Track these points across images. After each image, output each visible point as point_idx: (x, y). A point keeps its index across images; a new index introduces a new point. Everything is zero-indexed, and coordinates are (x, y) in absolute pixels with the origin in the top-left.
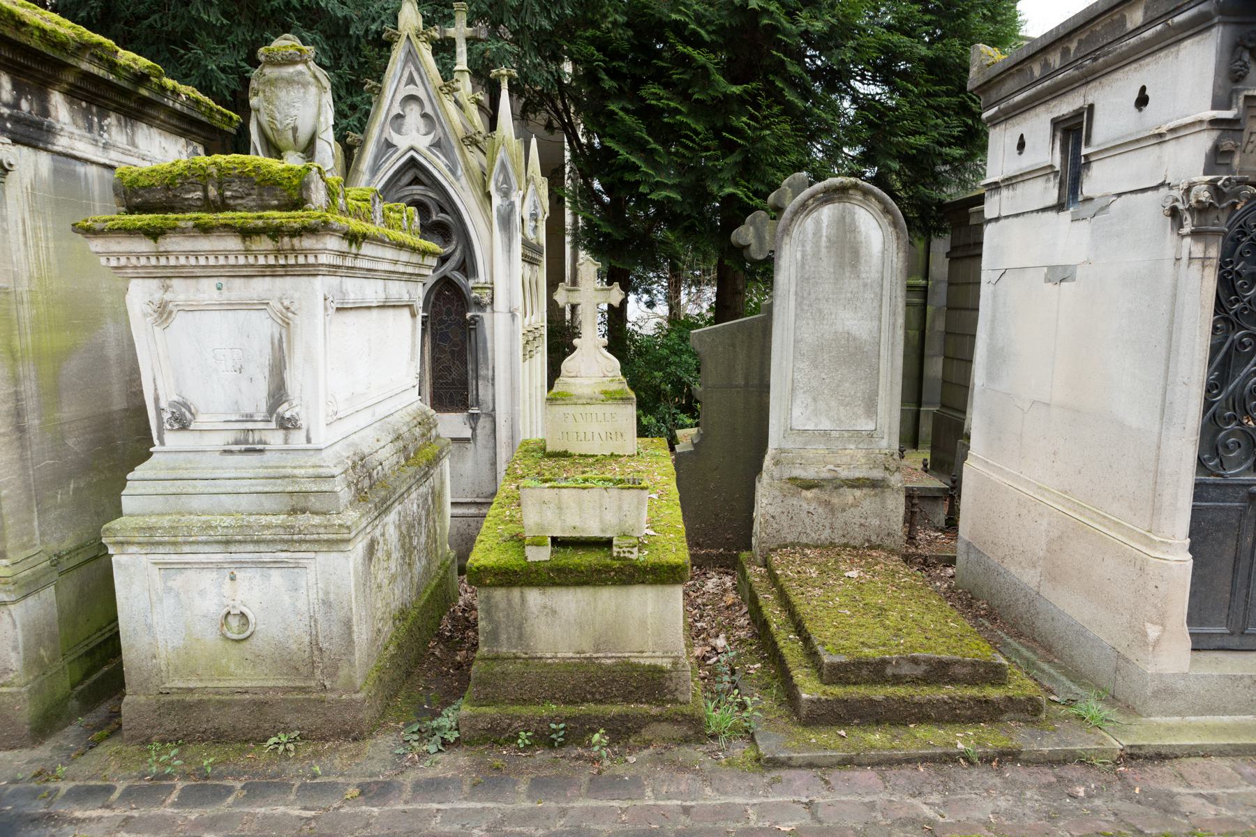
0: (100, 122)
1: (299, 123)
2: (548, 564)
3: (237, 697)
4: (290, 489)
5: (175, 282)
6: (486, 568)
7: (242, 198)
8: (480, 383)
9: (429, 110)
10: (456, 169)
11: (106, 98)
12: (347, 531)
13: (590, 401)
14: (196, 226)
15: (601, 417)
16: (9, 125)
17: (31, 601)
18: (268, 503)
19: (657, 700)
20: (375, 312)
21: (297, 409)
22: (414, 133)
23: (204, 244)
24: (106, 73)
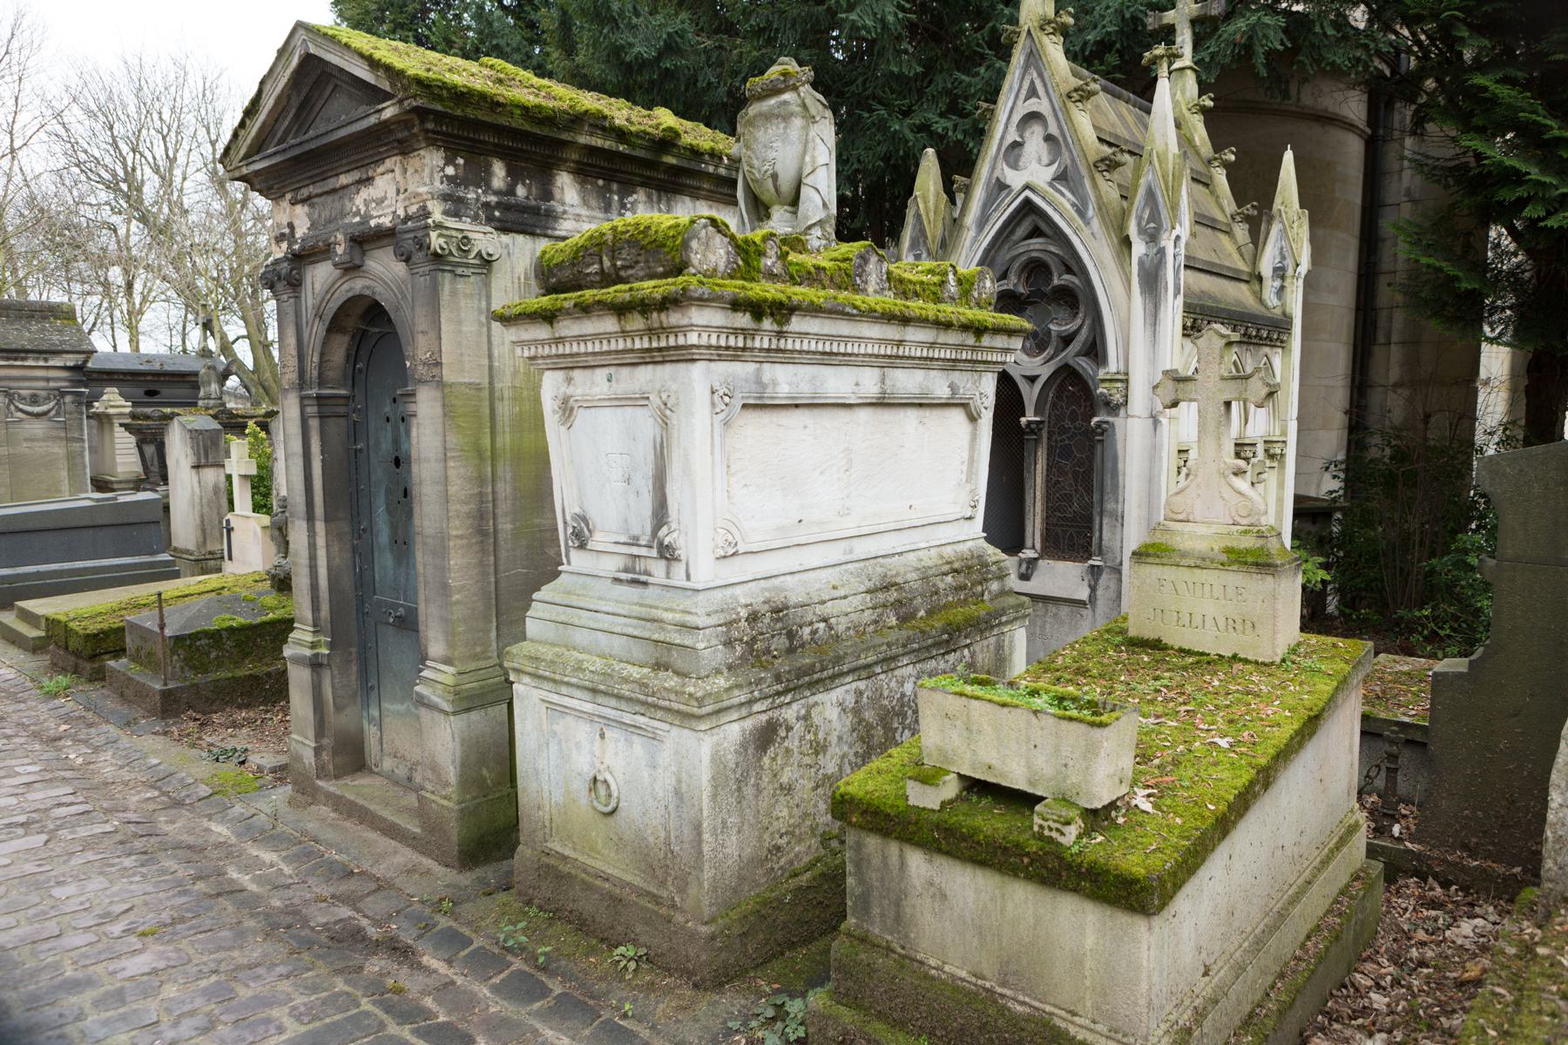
0: (621, 200)
1: (779, 168)
2: (935, 817)
3: (598, 882)
4: (656, 637)
5: (576, 374)
6: (852, 799)
7: (631, 267)
8: (1105, 521)
9: (1053, 129)
10: (1086, 209)
11: (630, 174)
12: (695, 704)
13: (1202, 562)
14: (576, 305)
15: (1218, 590)
16: (497, 214)
17: (475, 716)
18: (638, 651)
20: (864, 415)
21: (675, 535)
22: (1034, 166)
23: (589, 326)
24: (614, 144)
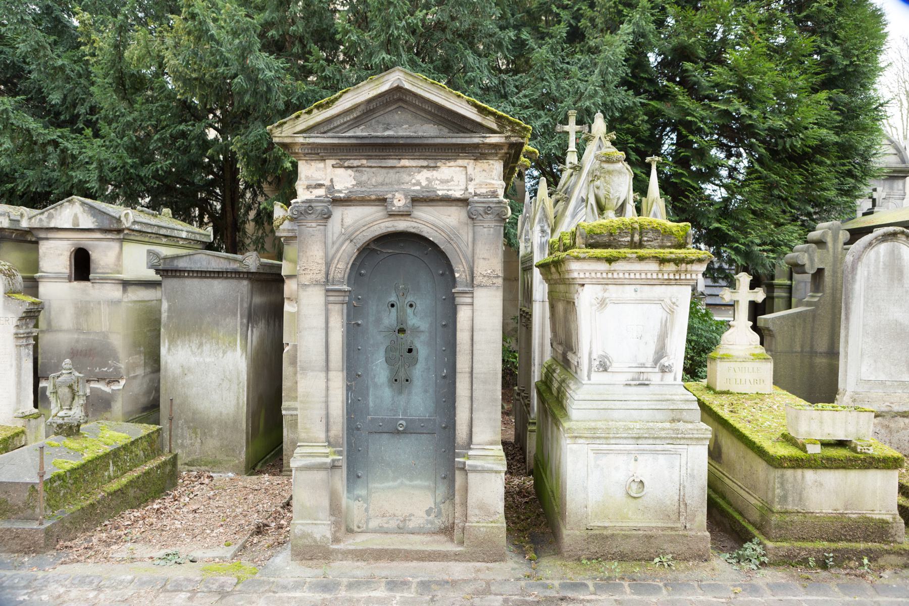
4: (671, 407)
15: (751, 370)
18: (659, 415)
19: (884, 541)
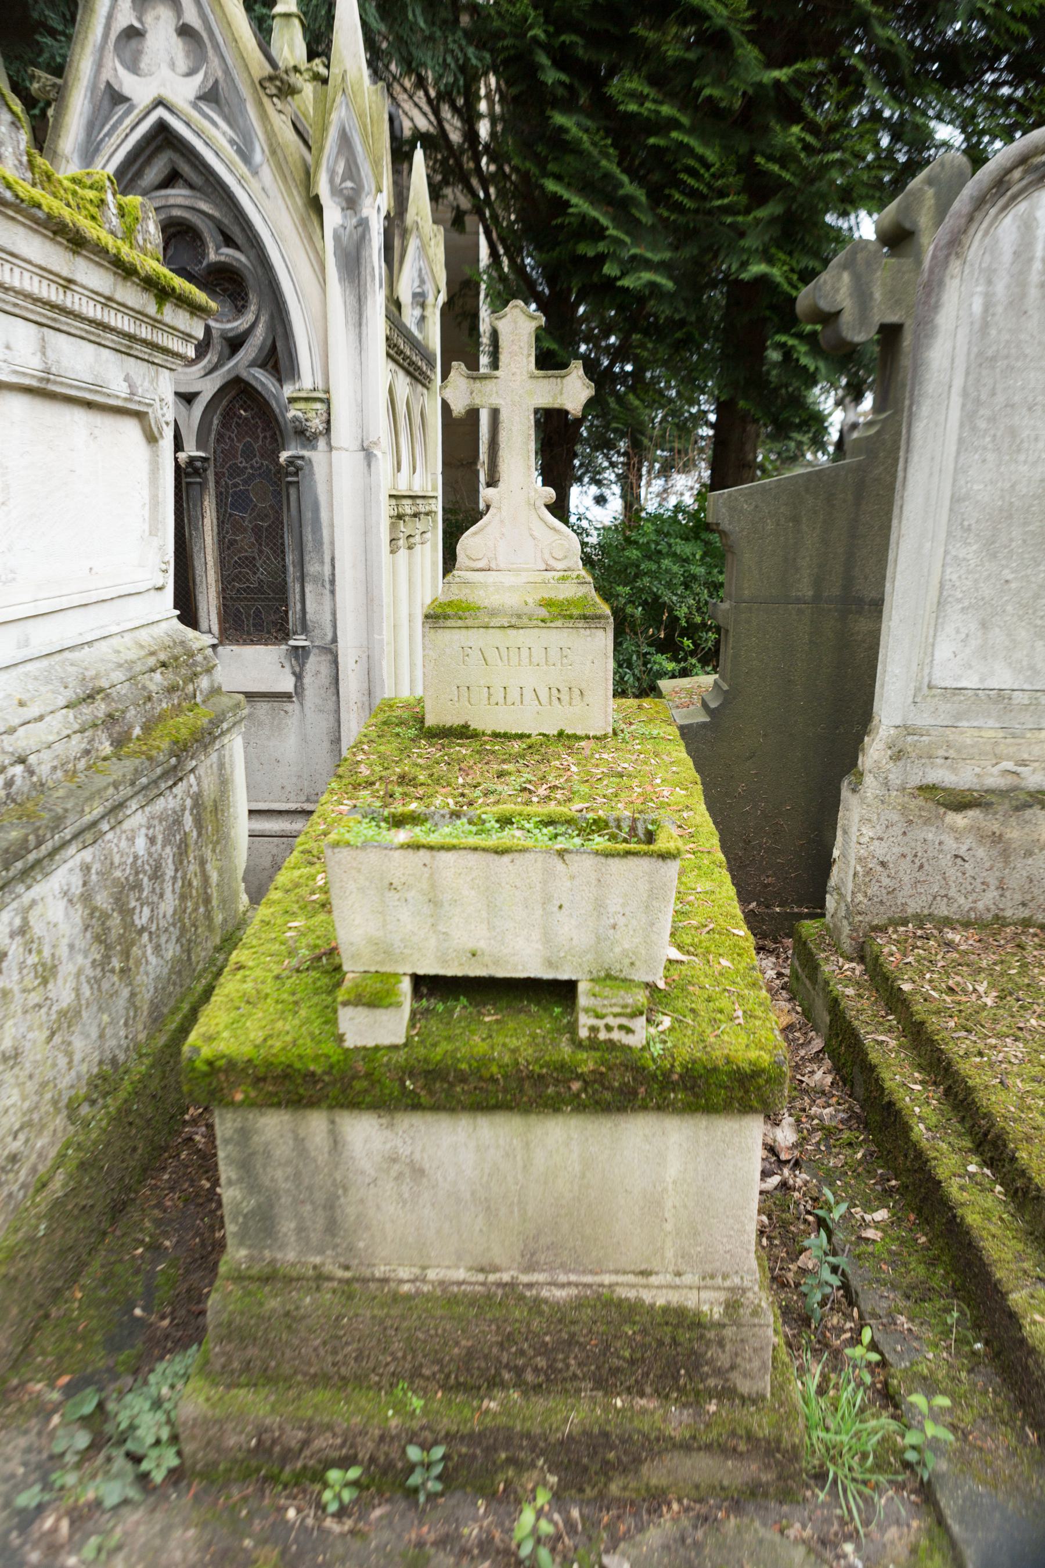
2: (401, 1057)
8: (308, 588)
9: (191, 17)
10: (252, 150)
13: (517, 622)
15: (538, 654)
19: (681, 1390)
22: (165, 71)
